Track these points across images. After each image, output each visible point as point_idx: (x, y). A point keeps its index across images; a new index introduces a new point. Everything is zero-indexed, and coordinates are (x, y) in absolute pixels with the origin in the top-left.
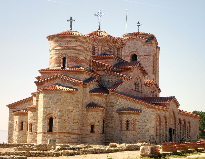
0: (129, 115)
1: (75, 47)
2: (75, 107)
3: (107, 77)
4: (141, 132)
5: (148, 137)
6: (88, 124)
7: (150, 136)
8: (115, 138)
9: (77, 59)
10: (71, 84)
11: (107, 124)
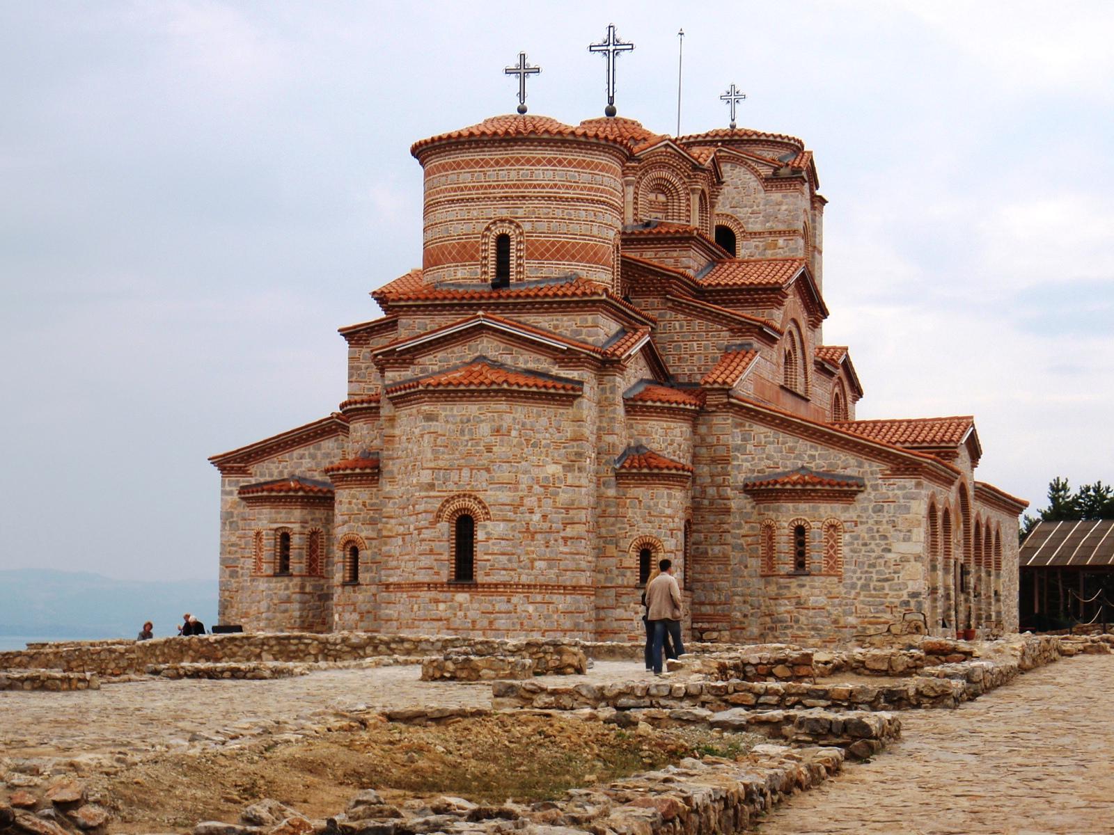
0: (807, 501)
1: (551, 188)
2: (569, 466)
3: (681, 326)
6: (624, 544)
7: (905, 598)
8: (740, 611)
9: (563, 245)
10: (549, 360)
11: (700, 543)
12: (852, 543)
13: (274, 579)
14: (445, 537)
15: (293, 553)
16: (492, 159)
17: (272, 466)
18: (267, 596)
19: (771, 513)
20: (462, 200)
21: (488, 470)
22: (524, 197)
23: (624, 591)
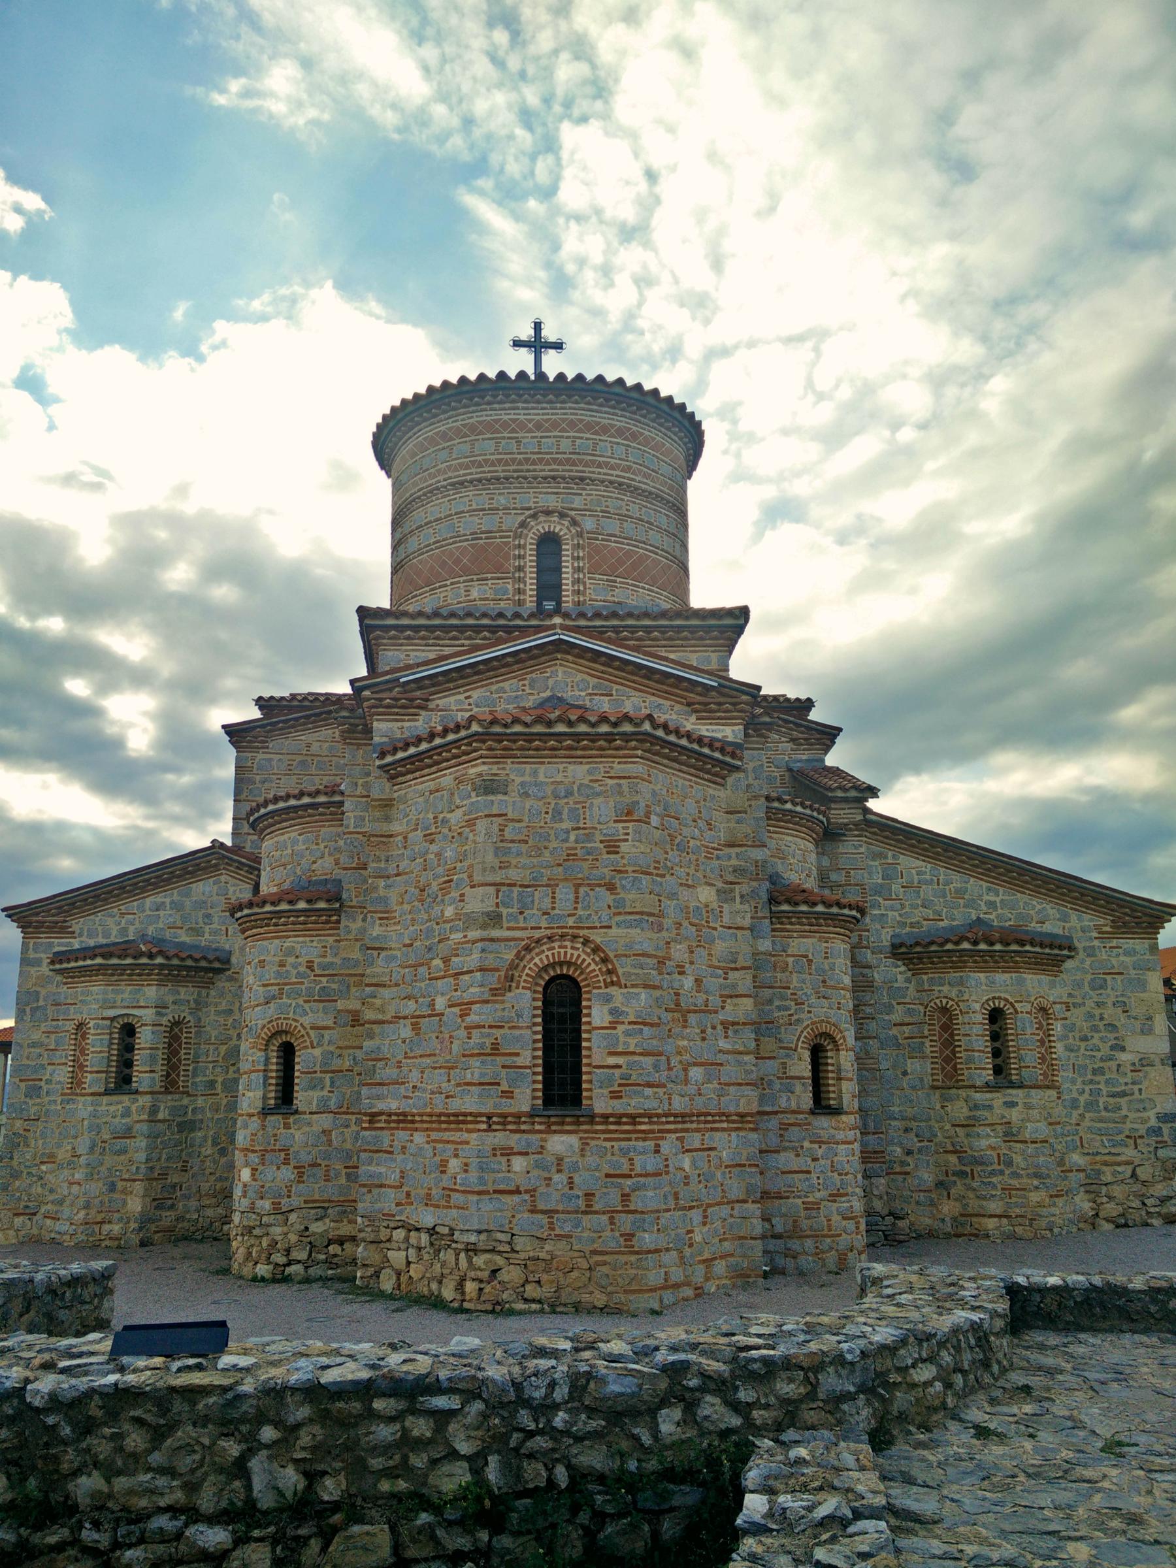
4: (1086, 1096)
5: (1143, 1132)
7: (1153, 1122)
8: (901, 1144)
9: (642, 559)
10: (677, 707)
12: (1066, 1037)
13: (105, 1099)
14: (526, 1021)
15: (139, 1057)
16: (530, 421)
17: (110, 922)
19: (946, 988)
20: (480, 480)
21: (611, 888)
22: (582, 479)
23: (791, 1119)
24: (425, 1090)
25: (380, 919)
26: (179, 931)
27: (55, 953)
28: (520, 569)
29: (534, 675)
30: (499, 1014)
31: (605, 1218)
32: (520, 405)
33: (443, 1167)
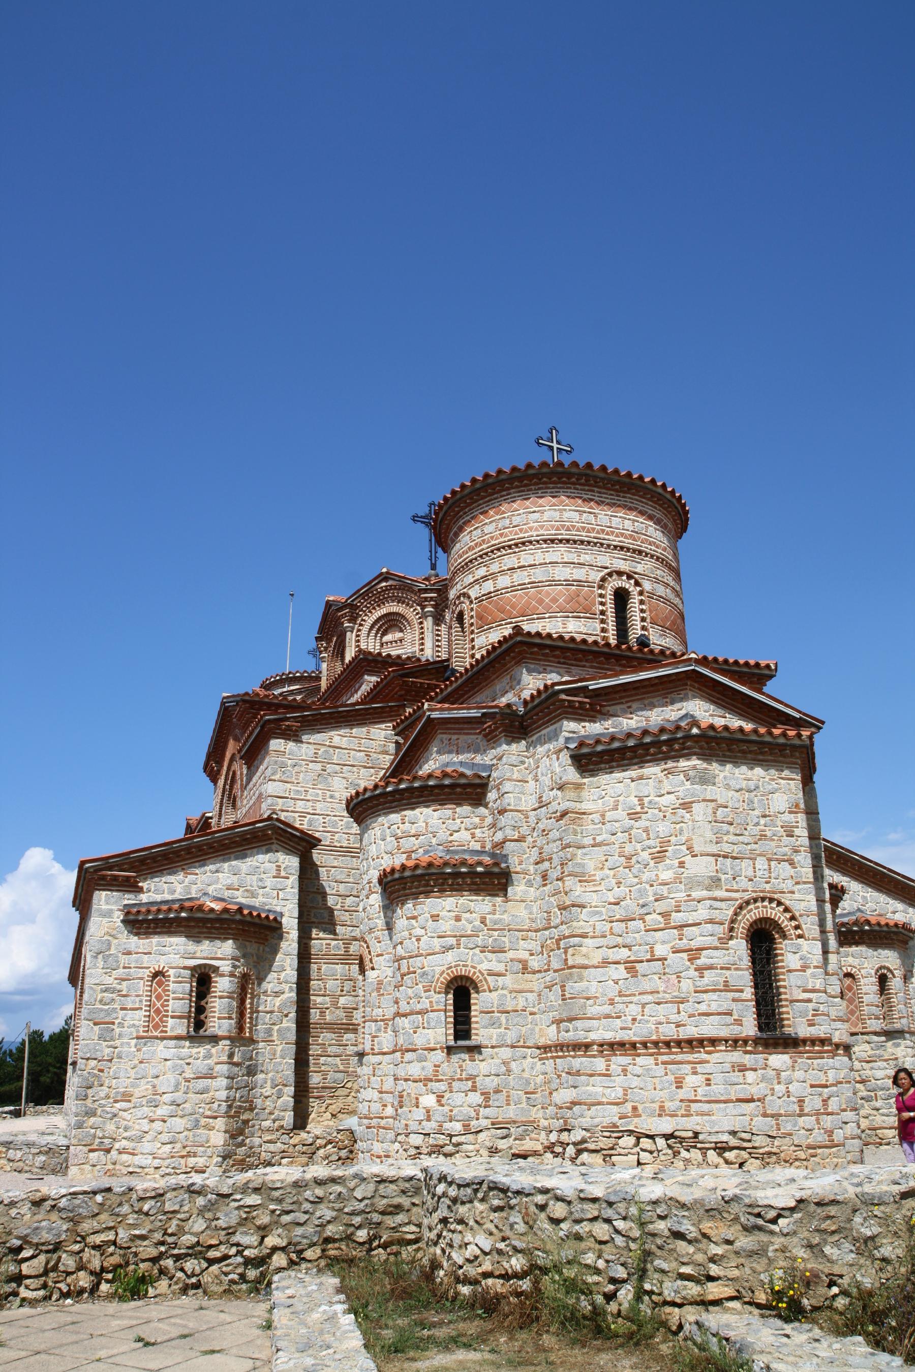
18: (175, 1067)
21: (792, 863)
22: (640, 552)
24: (647, 1022)
25: (580, 881)
26: (236, 892)
27: (125, 905)
28: (603, 613)
29: (672, 695)
30: (727, 958)
31: (814, 1118)
32: (596, 489)
33: (679, 1083)
